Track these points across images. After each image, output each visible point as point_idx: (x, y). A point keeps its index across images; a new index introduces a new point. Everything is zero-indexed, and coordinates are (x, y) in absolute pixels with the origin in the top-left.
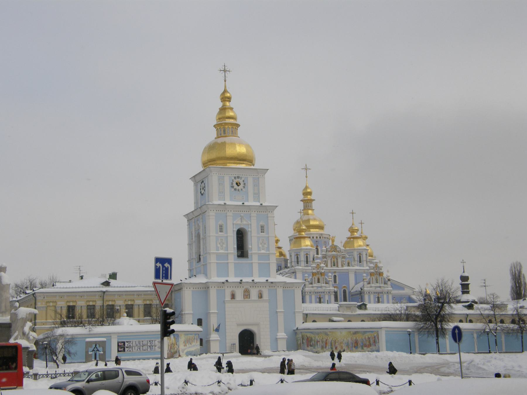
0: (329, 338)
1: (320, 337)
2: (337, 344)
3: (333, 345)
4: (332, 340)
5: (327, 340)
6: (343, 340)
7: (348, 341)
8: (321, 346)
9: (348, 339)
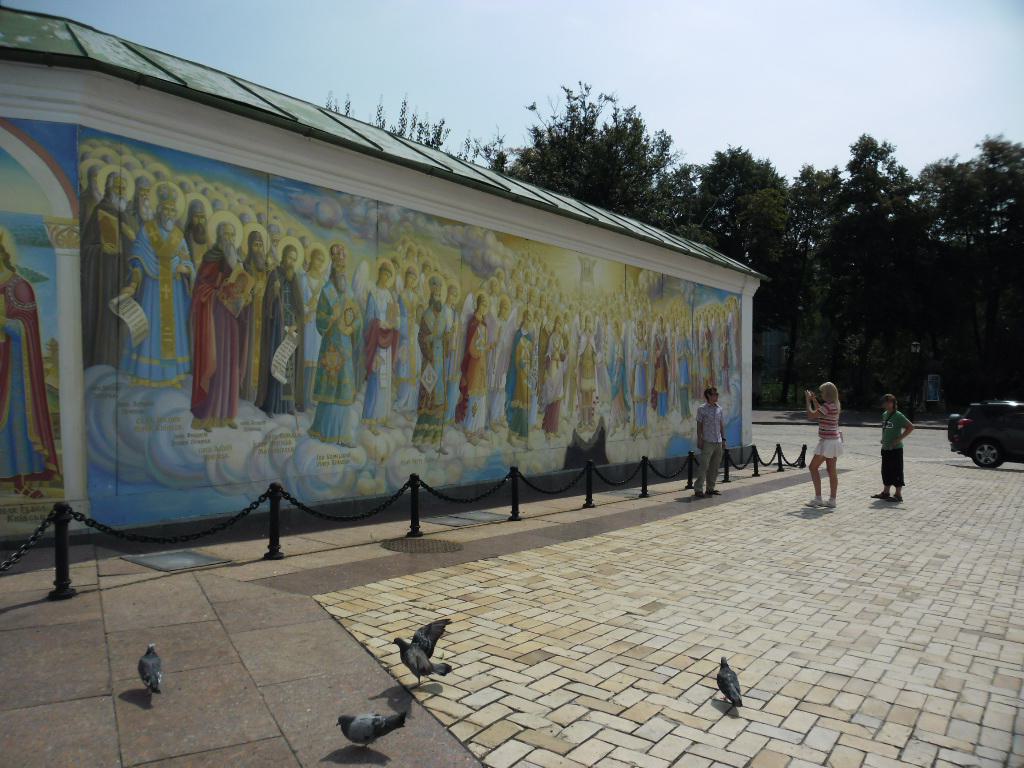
0: (494, 311)
1: (408, 273)
2: (556, 371)
3: (529, 383)
4: (517, 337)
5: (481, 330)
6: (597, 345)
7: (624, 344)
8: (411, 394)
9: (624, 325)
